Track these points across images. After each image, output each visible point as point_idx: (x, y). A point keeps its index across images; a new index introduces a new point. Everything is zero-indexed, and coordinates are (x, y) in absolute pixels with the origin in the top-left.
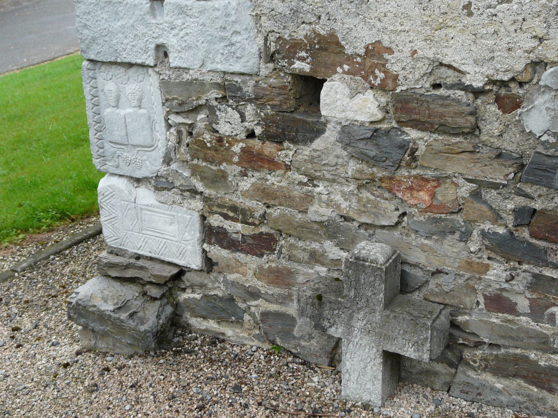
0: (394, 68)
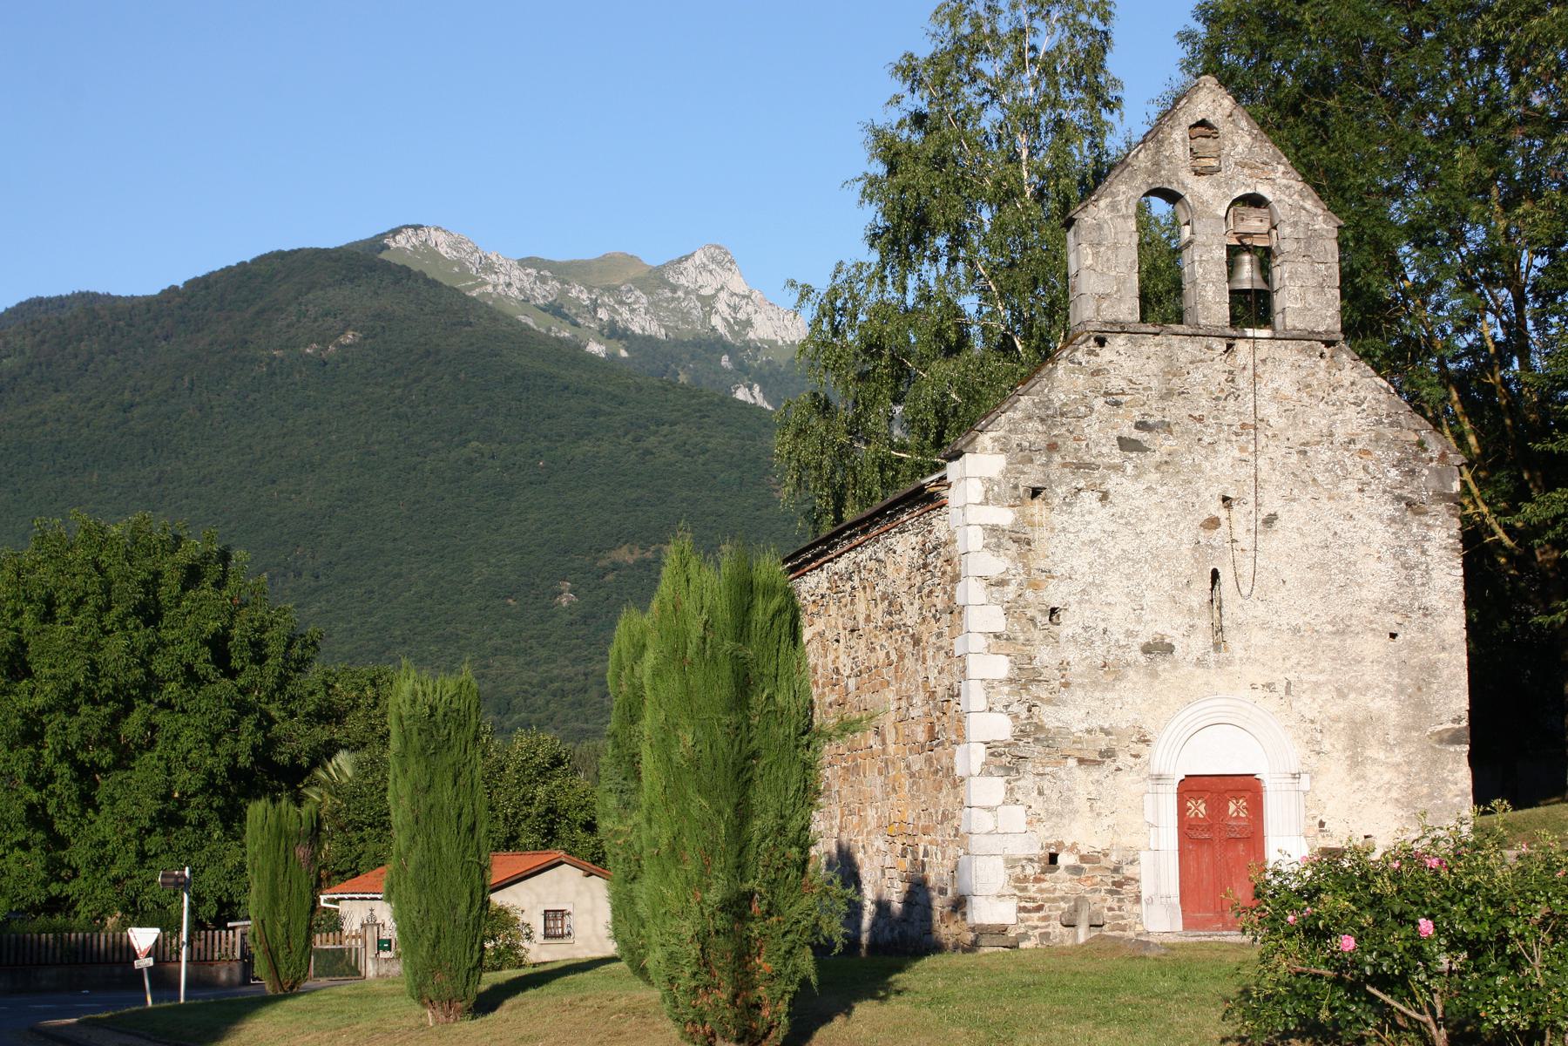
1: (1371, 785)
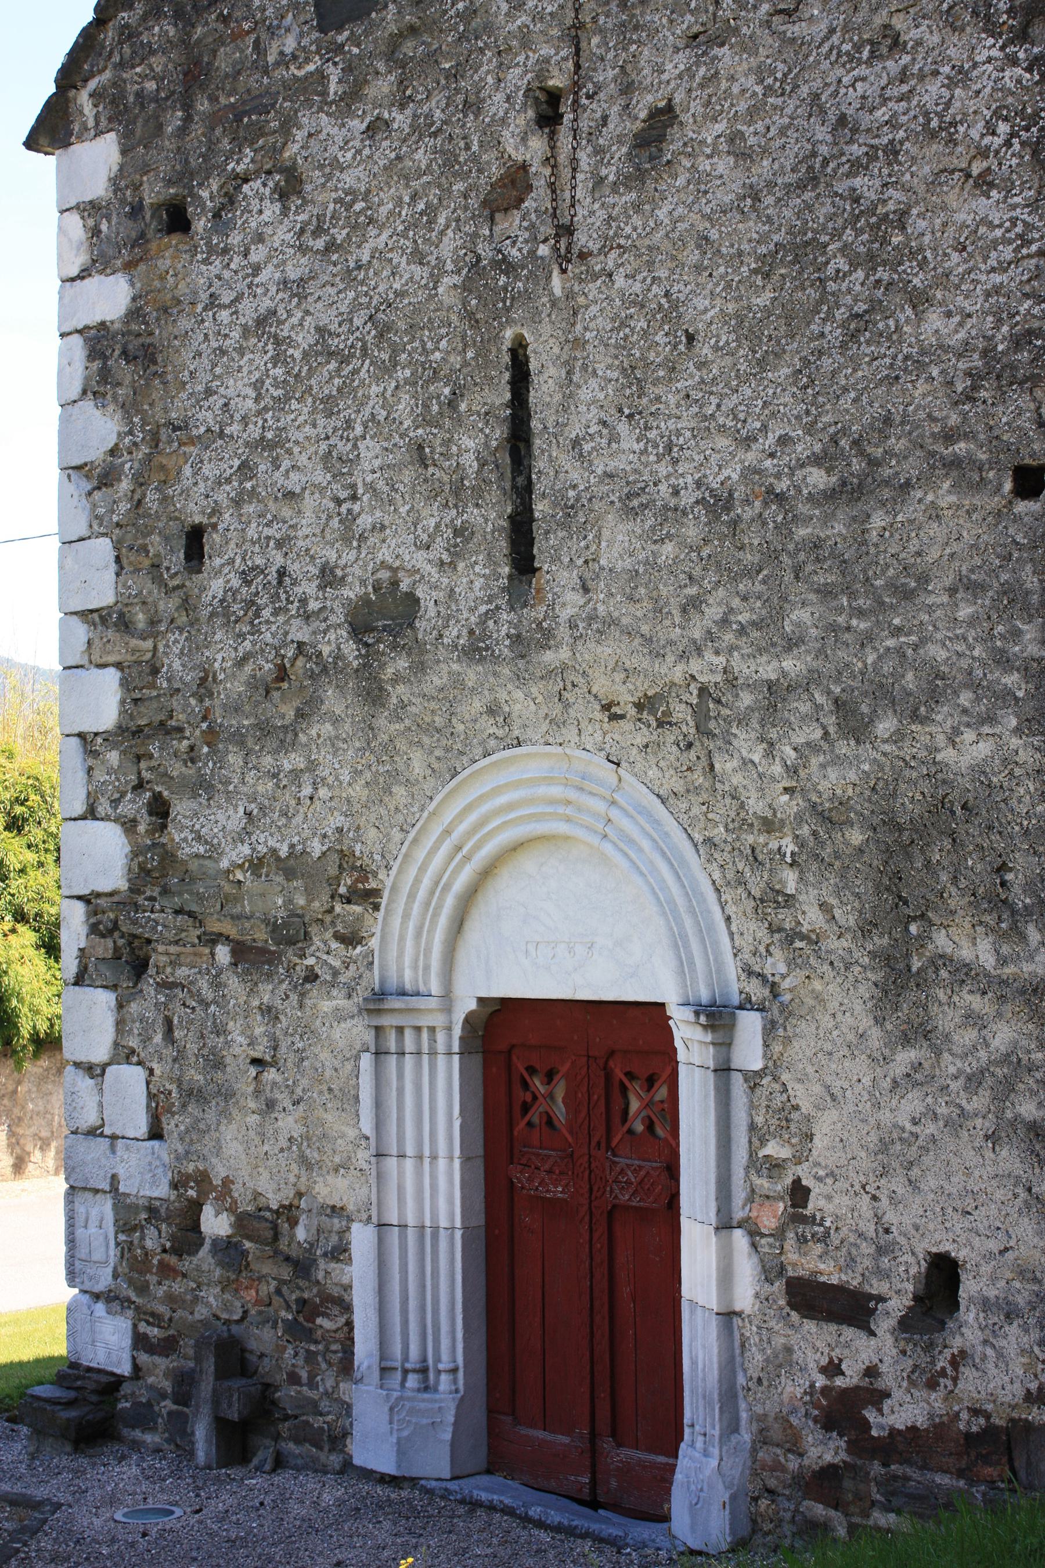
1: (950, 1065)
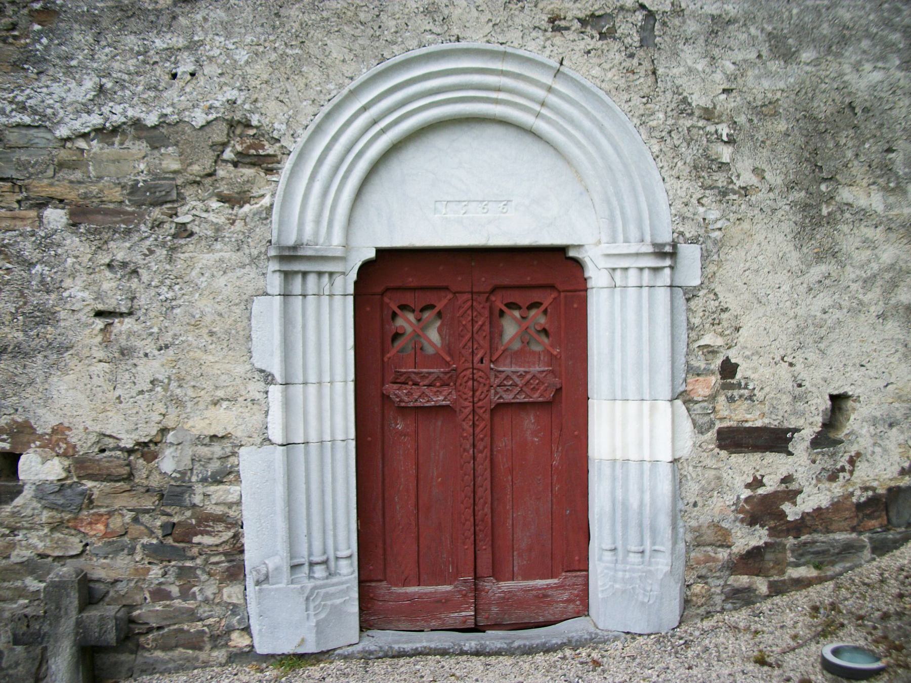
0: (73, 440)
1: (851, 273)
